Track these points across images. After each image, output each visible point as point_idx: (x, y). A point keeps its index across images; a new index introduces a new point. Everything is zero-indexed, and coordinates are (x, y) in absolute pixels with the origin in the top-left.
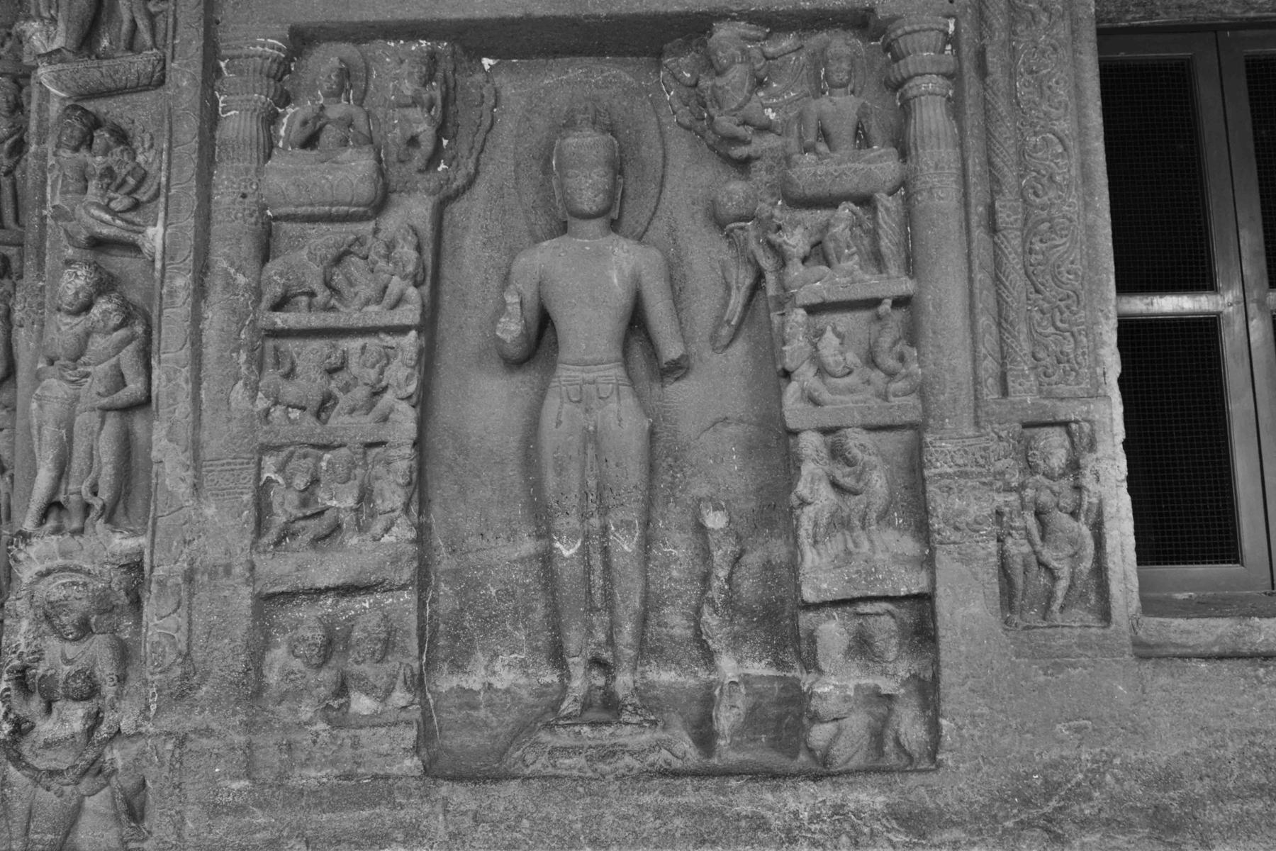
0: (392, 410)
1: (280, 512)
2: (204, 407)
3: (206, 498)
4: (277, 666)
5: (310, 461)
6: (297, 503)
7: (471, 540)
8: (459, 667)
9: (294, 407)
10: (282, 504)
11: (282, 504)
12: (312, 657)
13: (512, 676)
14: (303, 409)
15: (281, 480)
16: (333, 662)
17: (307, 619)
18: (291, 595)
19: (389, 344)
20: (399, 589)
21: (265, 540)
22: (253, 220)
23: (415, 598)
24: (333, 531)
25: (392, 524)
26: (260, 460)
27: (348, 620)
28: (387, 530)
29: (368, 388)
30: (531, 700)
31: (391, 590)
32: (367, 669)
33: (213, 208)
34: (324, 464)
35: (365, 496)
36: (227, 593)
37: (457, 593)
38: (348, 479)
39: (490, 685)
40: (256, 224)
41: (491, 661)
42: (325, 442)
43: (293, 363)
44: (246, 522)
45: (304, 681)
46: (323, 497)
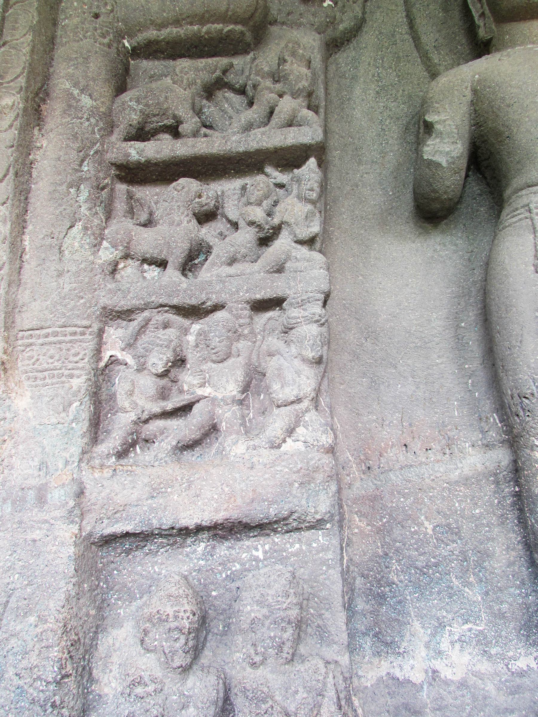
0: (288, 258)
1: (127, 404)
2: (26, 257)
3: (19, 383)
4: (115, 659)
5: (172, 333)
6: (152, 392)
7: (391, 454)
8: (387, 644)
9: (150, 264)
10: (131, 393)
11: (131, 393)
12: (174, 653)
13: (466, 658)
14: (162, 264)
15: (129, 360)
16: (207, 653)
17: (164, 580)
18: (141, 538)
19: (278, 181)
20: (311, 528)
21: (103, 448)
22: (106, 41)
23: (335, 542)
24: (206, 435)
25: (297, 423)
26: (101, 332)
27: (231, 578)
28: (290, 432)
29: (253, 230)
30: (502, 700)
31: (298, 529)
32: (269, 677)
33: (59, 33)
34: (191, 338)
35: (254, 382)
36: (37, 534)
37: (379, 531)
38: (228, 356)
39: (434, 671)
40: (109, 46)
41: (433, 635)
42: (194, 302)
43: (151, 214)
44: (75, 419)
45: (162, 696)
46: (188, 380)
